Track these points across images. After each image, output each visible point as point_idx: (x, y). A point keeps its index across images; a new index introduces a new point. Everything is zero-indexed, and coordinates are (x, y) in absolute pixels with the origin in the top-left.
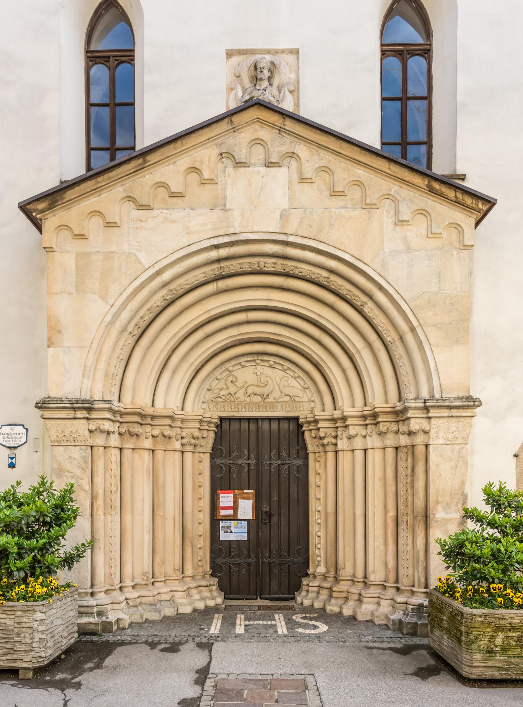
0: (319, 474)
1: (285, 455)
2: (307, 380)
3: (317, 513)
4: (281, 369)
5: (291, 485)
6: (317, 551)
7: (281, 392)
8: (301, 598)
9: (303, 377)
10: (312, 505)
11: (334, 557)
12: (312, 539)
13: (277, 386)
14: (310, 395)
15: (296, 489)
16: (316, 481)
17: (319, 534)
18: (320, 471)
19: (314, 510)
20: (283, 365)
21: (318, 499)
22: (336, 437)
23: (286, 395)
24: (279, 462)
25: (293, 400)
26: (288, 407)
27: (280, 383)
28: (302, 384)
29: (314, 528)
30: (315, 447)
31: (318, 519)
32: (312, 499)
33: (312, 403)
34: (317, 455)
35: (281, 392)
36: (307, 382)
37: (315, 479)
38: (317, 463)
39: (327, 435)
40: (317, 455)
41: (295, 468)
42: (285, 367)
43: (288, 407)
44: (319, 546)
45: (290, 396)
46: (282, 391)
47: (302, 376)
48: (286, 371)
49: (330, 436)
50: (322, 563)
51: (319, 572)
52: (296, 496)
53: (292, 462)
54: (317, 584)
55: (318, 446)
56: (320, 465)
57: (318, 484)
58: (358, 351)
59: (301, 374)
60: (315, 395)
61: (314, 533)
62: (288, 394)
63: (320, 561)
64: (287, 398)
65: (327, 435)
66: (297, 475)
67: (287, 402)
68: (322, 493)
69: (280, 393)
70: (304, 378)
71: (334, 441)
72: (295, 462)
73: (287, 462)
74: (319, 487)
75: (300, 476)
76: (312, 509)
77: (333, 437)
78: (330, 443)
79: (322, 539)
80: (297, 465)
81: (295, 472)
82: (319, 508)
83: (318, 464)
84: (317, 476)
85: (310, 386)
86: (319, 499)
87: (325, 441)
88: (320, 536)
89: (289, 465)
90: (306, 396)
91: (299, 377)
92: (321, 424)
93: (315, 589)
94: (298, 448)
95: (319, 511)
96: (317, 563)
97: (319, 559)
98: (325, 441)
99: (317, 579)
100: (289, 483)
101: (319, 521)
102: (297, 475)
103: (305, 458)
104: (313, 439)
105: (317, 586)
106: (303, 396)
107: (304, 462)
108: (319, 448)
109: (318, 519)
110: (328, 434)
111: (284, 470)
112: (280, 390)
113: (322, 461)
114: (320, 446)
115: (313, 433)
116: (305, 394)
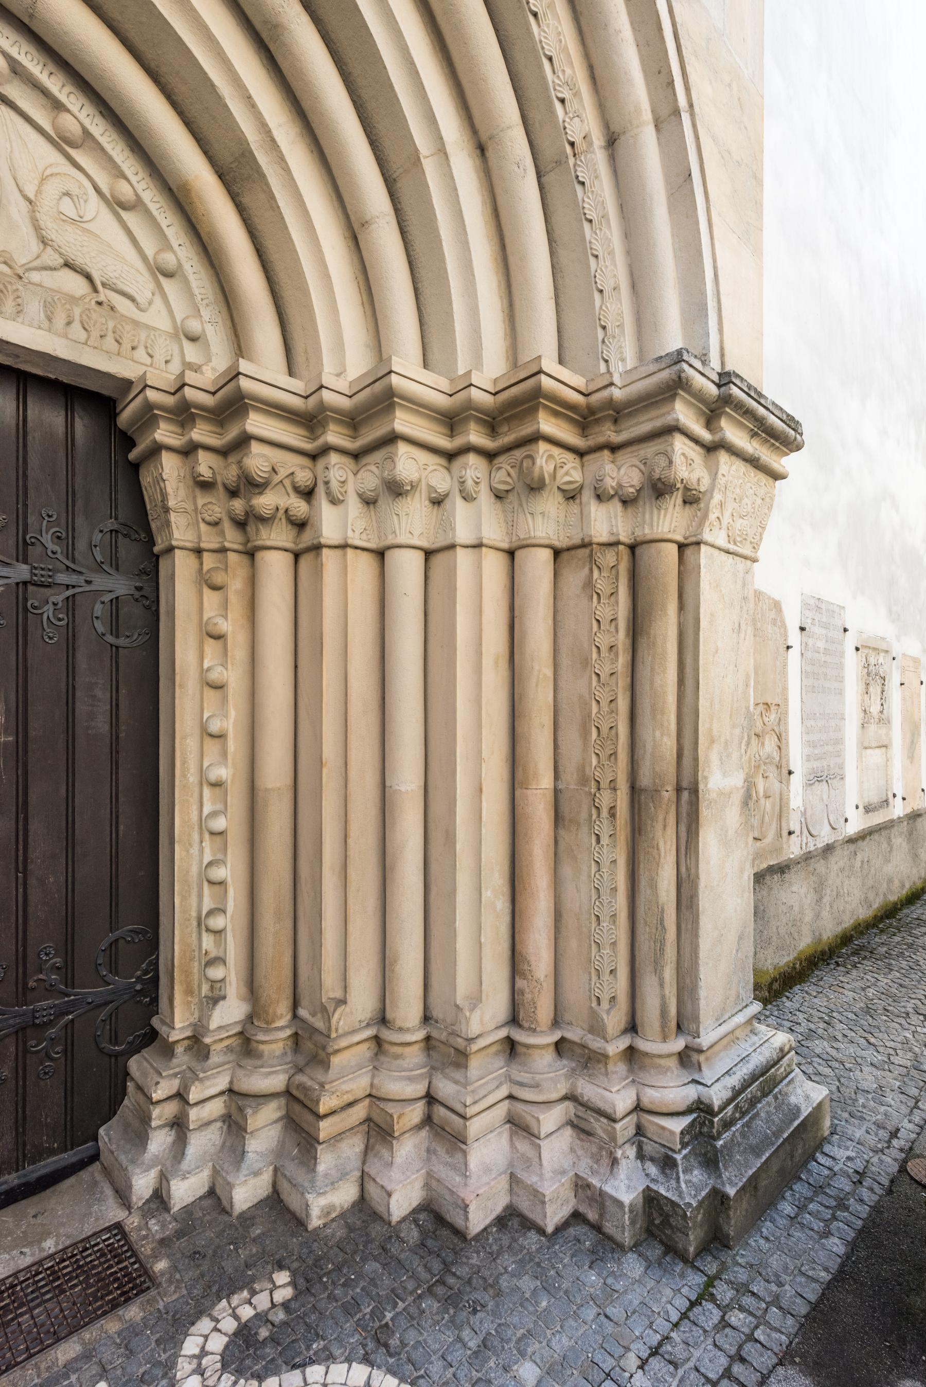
0: (218, 637)
1: (51, 546)
2: (175, 232)
3: (207, 792)
4: (48, 127)
5: (83, 679)
6: (208, 942)
7: (44, 241)
8: (153, 1174)
9: (155, 213)
10: (184, 763)
11: (287, 959)
12: (184, 899)
13: (24, 204)
14: (180, 309)
15: (102, 694)
16: (206, 665)
17: (219, 873)
18: (224, 626)
19: (193, 779)
20: (57, 106)
21: (212, 736)
22: (308, 494)
23: (67, 265)
24: (22, 571)
25: (102, 298)
26: (76, 325)
27: (38, 192)
28: (150, 252)
29: (195, 850)
30: (203, 526)
31: (214, 814)
32: (184, 738)
33: (188, 346)
34: (209, 561)
35: (44, 241)
36: (175, 244)
37: (201, 658)
38: (207, 592)
39: (277, 479)
40: (209, 561)
41: (98, 609)
42: (69, 123)
43: (76, 325)
44: (217, 922)
45: (88, 277)
46: (52, 235)
47: (153, 207)
48: (72, 152)
49: (287, 483)
50: (234, 989)
51: (220, 1028)
52: (102, 725)
53: (89, 582)
54: (222, 1083)
55: (215, 524)
56: (225, 605)
57: (216, 675)
58: (441, 150)
59: (151, 197)
60: (206, 314)
61: (194, 870)
62: (80, 260)
63: (223, 980)
64: (74, 284)
65: (277, 479)
66: (110, 639)
67: (73, 300)
68: (232, 713)
69: (34, 246)
70: (164, 223)
71: (299, 507)
72: (100, 582)
73: (62, 578)
74: (219, 687)
75: (121, 642)
76: (184, 776)
77: (297, 490)
78: (281, 512)
79: (235, 899)
80: (107, 598)
81: (100, 627)
82: (221, 773)
83: (211, 599)
84: (211, 647)
85: (187, 266)
86: (220, 737)
87: (266, 502)
88: (222, 883)
89: (70, 592)
90: (164, 312)
91: (137, 205)
92: (256, 423)
93: (216, 1108)
94: (111, 524)
95: (217, 785)
96: (205, 988)
97: (216, 973)
98: (266, 502)
99: (215, 1059)
100: (71, 670)
101: (220, 824)
102: (110, 639)
103: (144, 572)
104: (198, 492)
105: (222, 1093)
106: (150, 303)
107: (139, 589)
108: (222, 533)
109: (214, 814)
110: (283, 473)
111: (48, 610)
112: (37, 228)
113: (236, 584)
114: (227, 525)
115: (205, 464)
116: (158, 301)
